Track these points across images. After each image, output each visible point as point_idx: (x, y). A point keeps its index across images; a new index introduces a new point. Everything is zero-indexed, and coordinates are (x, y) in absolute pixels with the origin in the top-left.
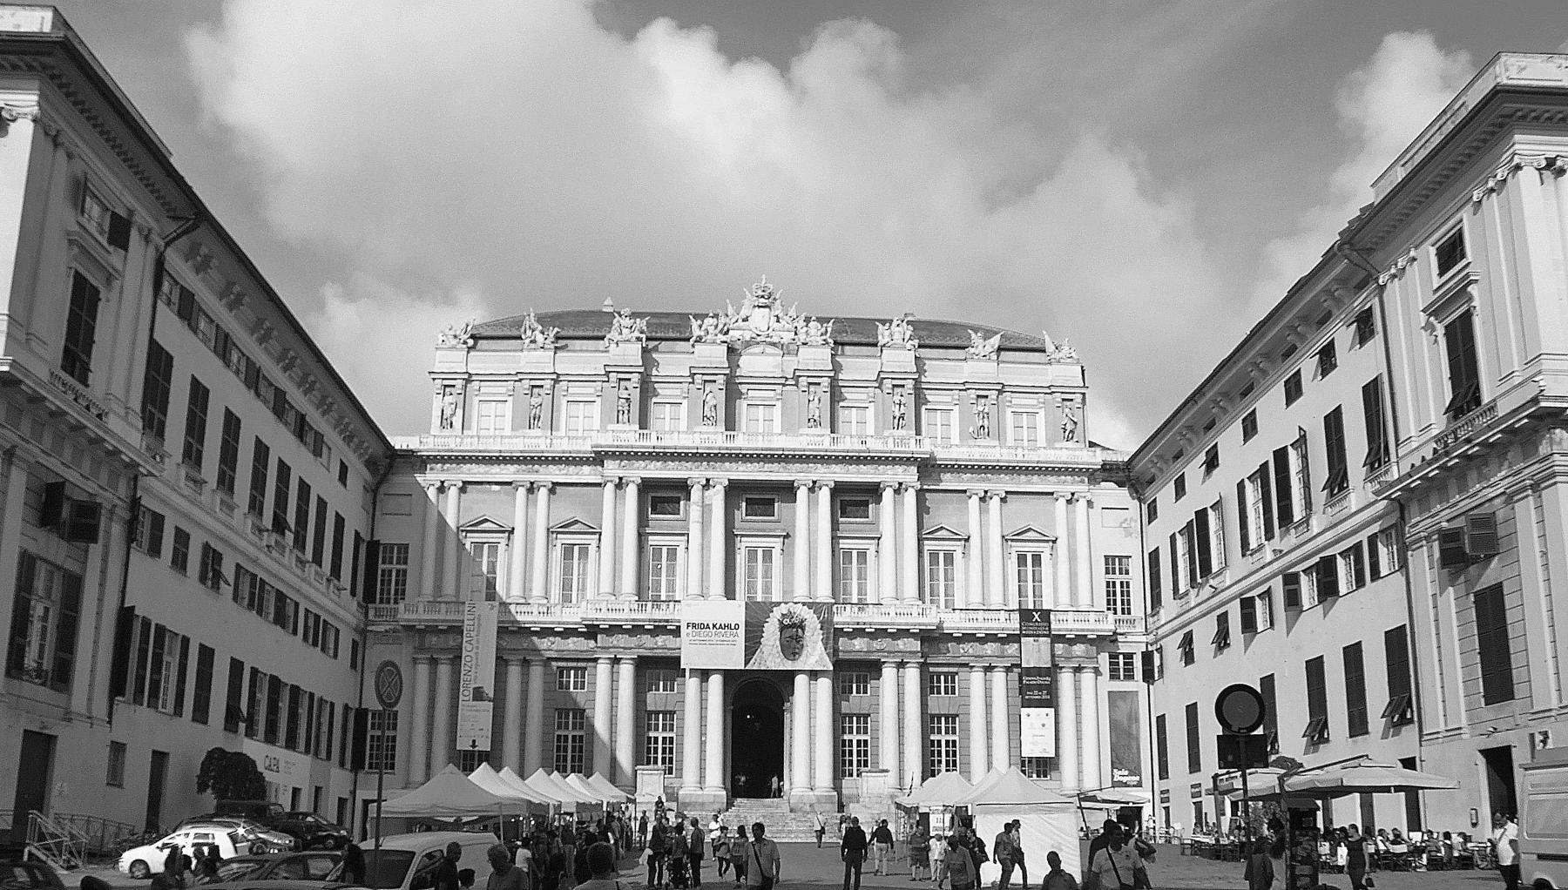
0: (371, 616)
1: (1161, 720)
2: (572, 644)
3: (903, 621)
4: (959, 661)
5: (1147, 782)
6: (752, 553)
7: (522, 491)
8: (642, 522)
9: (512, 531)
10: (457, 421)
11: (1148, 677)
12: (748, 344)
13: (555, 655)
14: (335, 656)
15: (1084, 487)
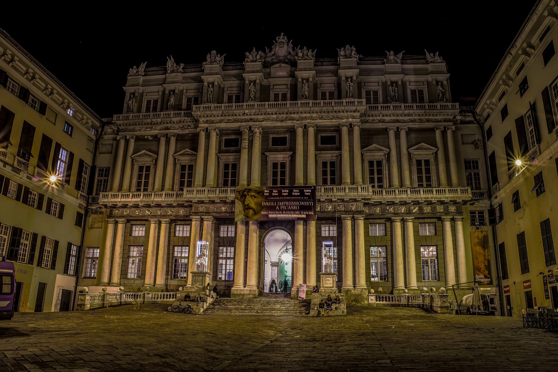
0: (90, 201)
1: (502, 246)
2: (182, 212)
3: (353, 195)
4: (386, 216)
5: (495, 282)
6: (275, 165)
7: (163, 140)
8: (220, 151)
9: (156, 160)
10: (135, 109)
11: (493, 222)
12: (274, 63)
13: (174, 218)
14: (61, 216)
15: (451, 123)
